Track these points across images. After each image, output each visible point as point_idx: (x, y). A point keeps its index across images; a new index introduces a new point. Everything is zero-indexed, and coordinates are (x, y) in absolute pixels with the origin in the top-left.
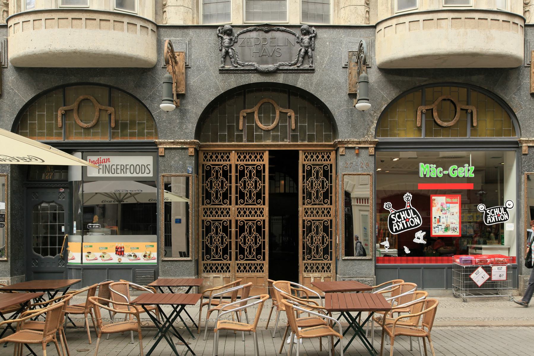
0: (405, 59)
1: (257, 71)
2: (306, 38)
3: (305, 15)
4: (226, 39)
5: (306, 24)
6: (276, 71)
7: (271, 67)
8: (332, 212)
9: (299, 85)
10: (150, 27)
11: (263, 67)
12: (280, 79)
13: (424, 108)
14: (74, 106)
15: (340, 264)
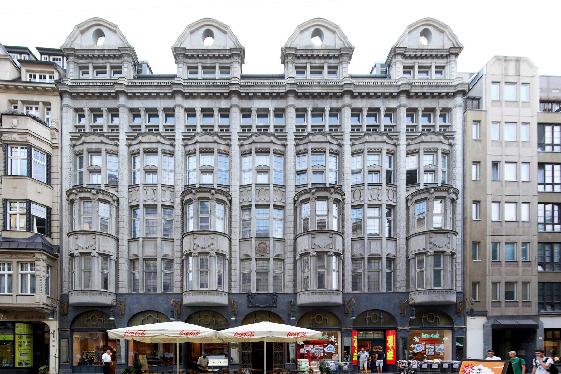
0: (305, 304)
1: (259, 307)
2: (275, 297)
3: (274, 289)
4: (250, 297)
5: (275, 293)
6: (265, 307)
7: (264, 306)
8: (283, 350)
9: (272, 311)
10: (227, 294)
11: (261, 306)
12: (266, 309)
13: (312, 318)
14: (203, 318)
15: (286, 366)
